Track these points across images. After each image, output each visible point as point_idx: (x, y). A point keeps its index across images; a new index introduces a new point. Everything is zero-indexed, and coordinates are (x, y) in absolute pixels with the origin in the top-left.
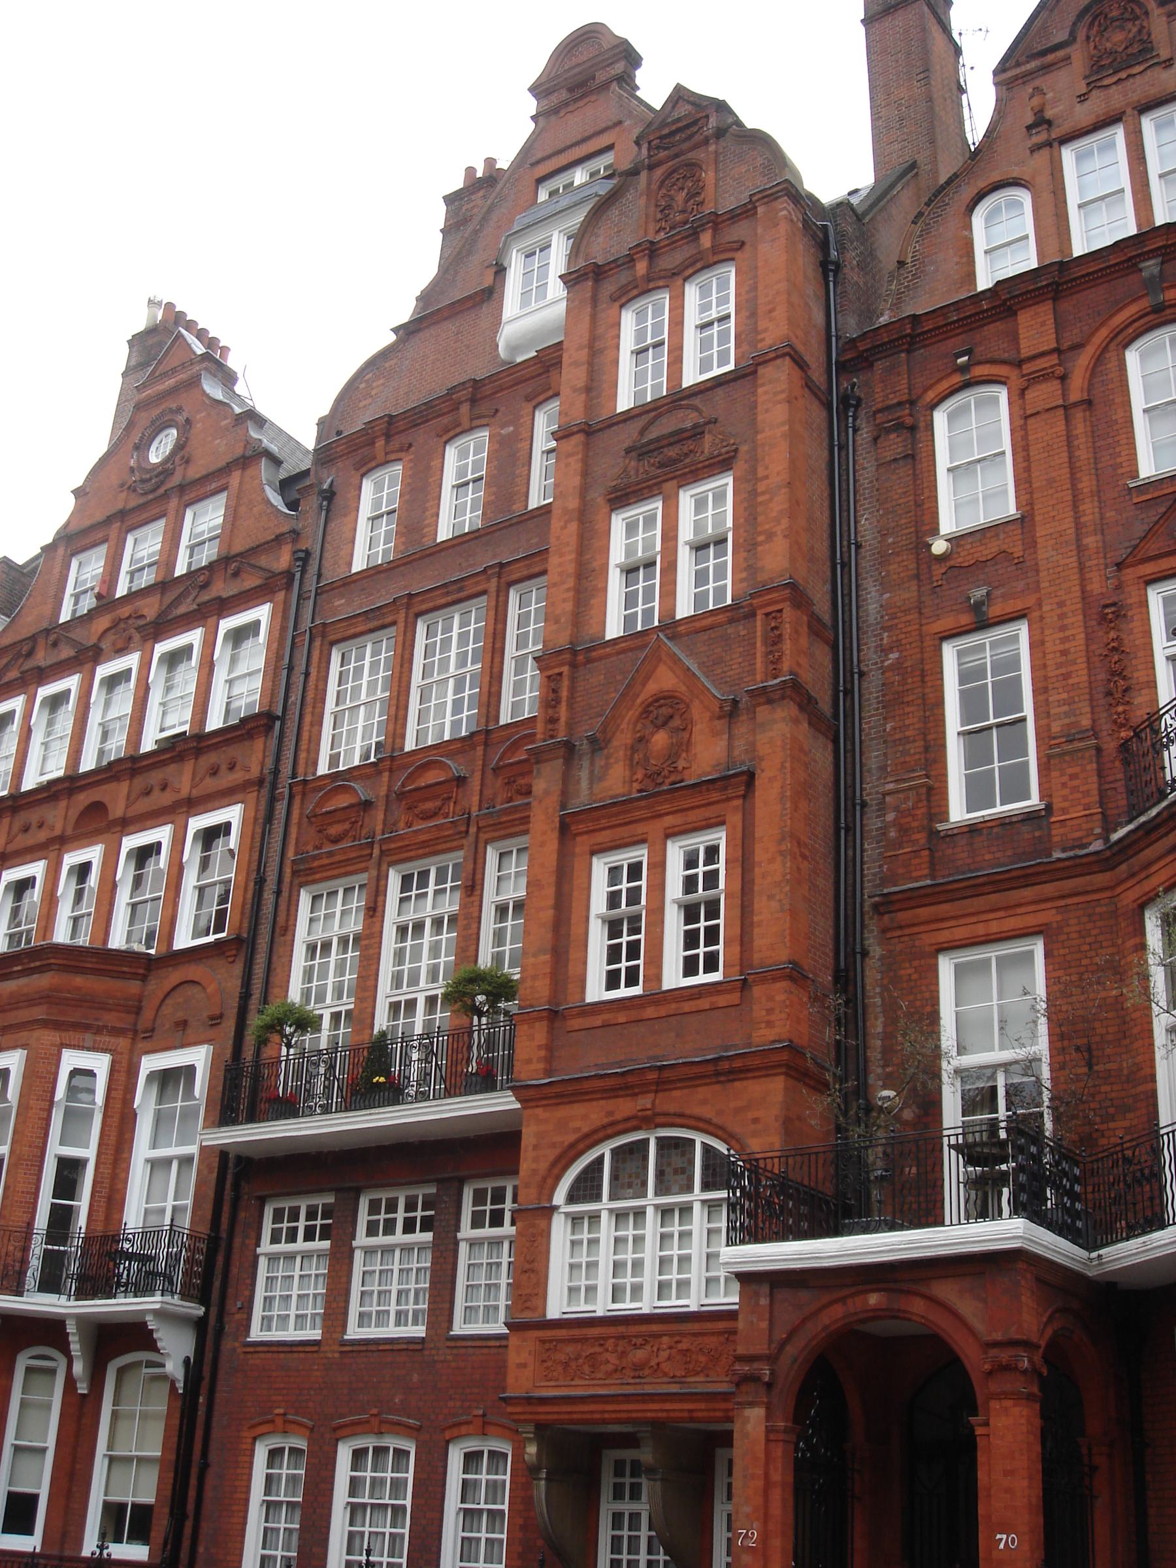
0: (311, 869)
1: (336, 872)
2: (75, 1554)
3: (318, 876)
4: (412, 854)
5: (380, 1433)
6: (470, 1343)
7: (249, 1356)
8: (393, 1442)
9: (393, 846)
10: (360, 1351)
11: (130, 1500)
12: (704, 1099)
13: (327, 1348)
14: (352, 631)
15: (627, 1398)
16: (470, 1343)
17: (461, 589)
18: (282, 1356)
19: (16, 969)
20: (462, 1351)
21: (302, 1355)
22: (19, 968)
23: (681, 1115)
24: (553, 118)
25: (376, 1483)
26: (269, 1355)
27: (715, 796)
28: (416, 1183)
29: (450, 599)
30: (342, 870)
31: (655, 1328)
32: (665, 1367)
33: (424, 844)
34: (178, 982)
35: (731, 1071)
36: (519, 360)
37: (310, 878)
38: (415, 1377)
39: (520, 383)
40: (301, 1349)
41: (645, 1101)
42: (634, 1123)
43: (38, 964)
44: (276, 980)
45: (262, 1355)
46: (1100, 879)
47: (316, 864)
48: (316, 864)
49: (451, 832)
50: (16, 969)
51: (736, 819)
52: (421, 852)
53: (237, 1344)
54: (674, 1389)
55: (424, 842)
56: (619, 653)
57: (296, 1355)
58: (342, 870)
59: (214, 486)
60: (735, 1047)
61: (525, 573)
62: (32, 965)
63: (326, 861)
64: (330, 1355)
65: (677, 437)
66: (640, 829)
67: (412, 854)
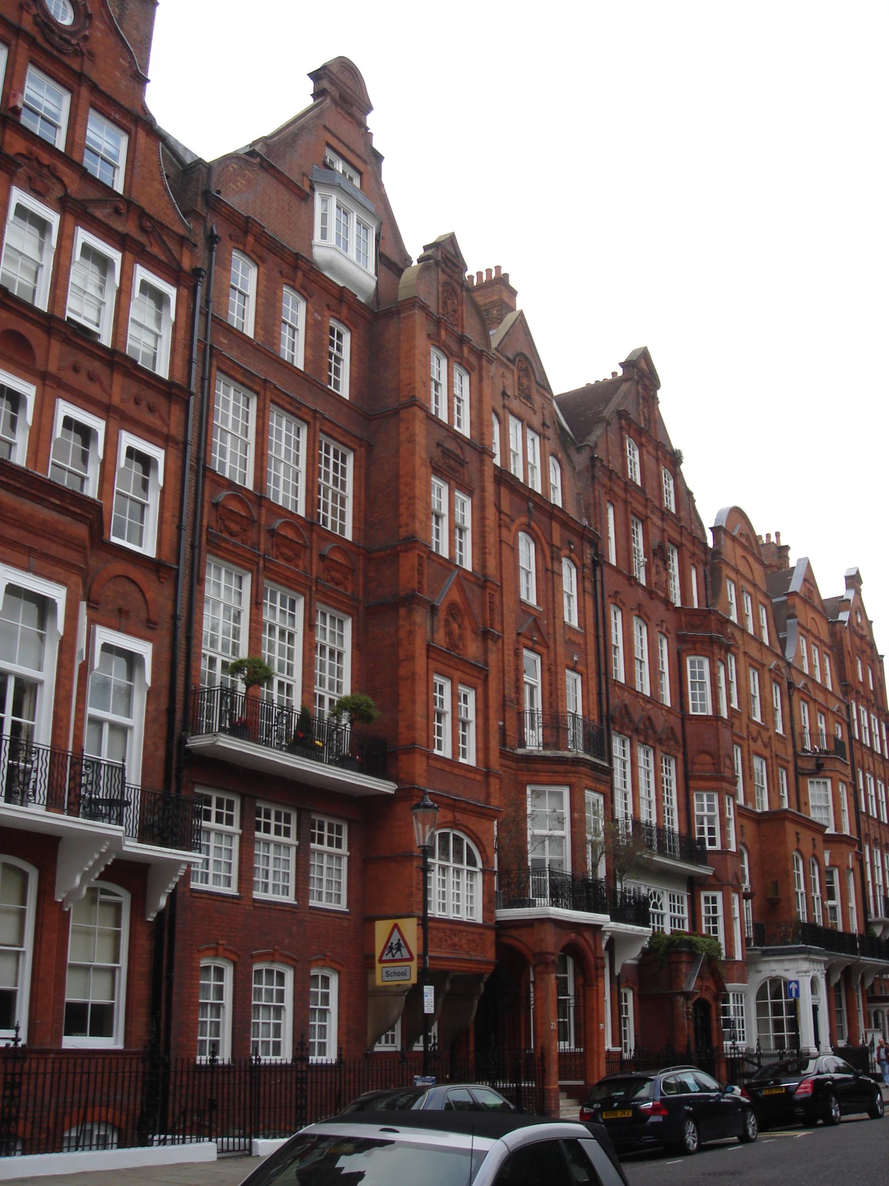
0: (219, 545)
1: (233, 559)
2: (55, 1047)
3: (220, 553)
4: (277, 578)
5: (273, 961)
6: (321, 913)
7: (196, 900)
8: (277, 967)
9: (272, 567)
10: (265, 908)
11: (91, 1000)
12: (472, 822)
13: (245, 903)
14: (232, 373)
15: (455, 960)
16: (321, 913)
17: (298, 409)
18: (218, 903)
19: (52, 500)
20: (317, 917)
21: (230, 905)
22: (58, 502)
23: (467, 827)
24: (334, 106)
25: (269, 992)
26: (209, 901)
27: (476, 674)
28: (274, 802)
29: (292, 409)
30: (237, 560)
31: (461, 928)
32: (464, 946)
33: (287, 578)
34: (121, 573)
35: (484, 814)
36: (327, 274)
37: (215, 551)
38: (295, 929)
39: (326, 291)
40: (231, 900)
41: (458, 816)
42: (451, 825)
43: (78, 511)
44: (195, 617)
45: (204, 901)
46: (513, 765)
47: (224, 545)
48: (224, 545)
49: (303, 581)
50: (52, 500)
51: (480, 689)
52: (284, 581)
53: (186, 889)
54: (467, 957)
55: (288, 577)
56: (439, 564)
57: (226, 904)
58: (237, 560)
59: (117, 116)
60: (479, 801)
61: (330, 432)
62: (72, 508)
63: (231, 548)
64: (247, 907)
65: (456, 458)
66: (452, 672)
67: (277, 578)
